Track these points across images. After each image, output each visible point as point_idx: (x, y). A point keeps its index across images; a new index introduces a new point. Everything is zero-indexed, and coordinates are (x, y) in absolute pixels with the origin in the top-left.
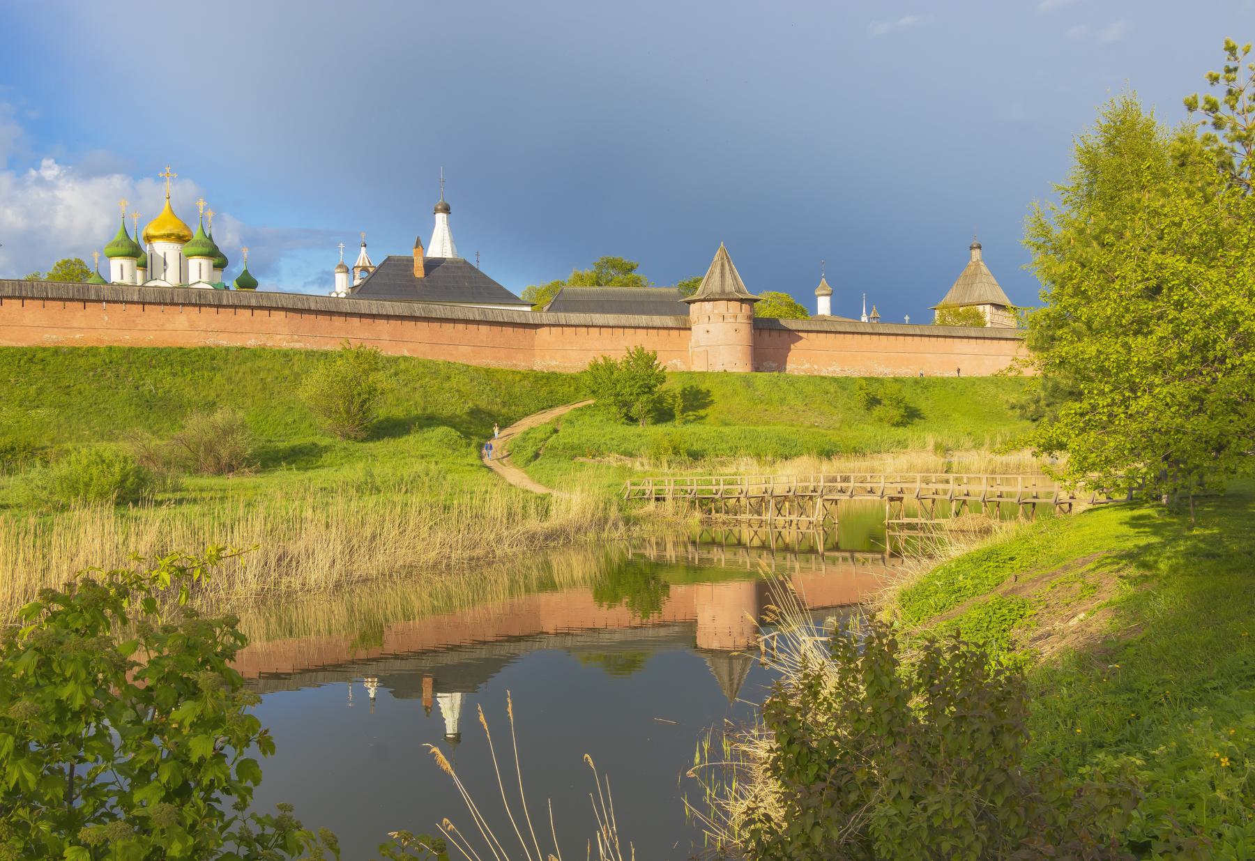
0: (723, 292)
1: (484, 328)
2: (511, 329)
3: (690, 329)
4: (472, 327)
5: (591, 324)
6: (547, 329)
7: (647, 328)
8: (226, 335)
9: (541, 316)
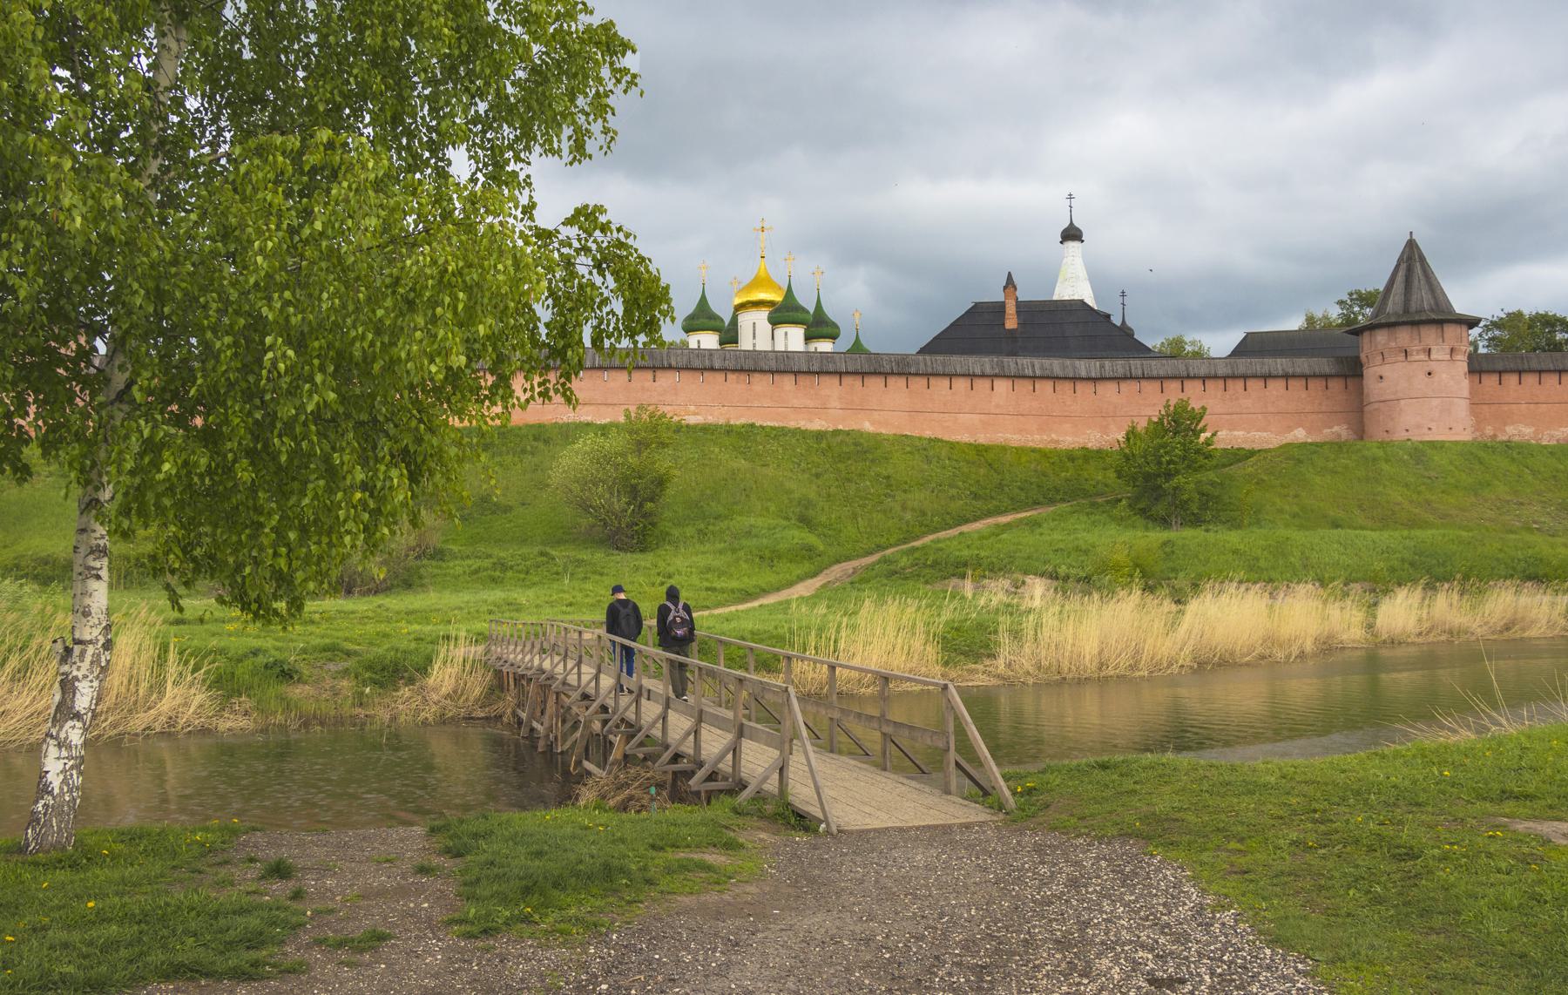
0: (1406, 311)
1: (1002, 386)
3: (1362, 376)
7: (1286, 377)
8: (592, 408)
9: (1102, 367)
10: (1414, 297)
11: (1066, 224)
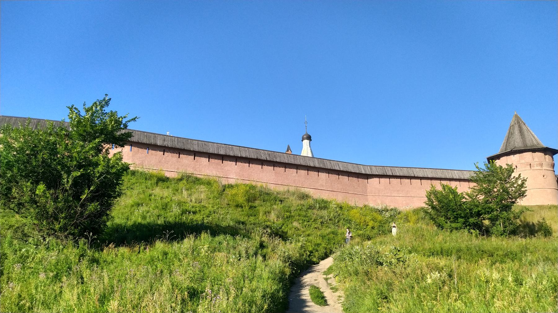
1: (323, 175)
2: (346, 178)
4: (313, 174)
5: (413, 175)
6: (376, 180)
10: (527, 140)
11: (305, 133)
